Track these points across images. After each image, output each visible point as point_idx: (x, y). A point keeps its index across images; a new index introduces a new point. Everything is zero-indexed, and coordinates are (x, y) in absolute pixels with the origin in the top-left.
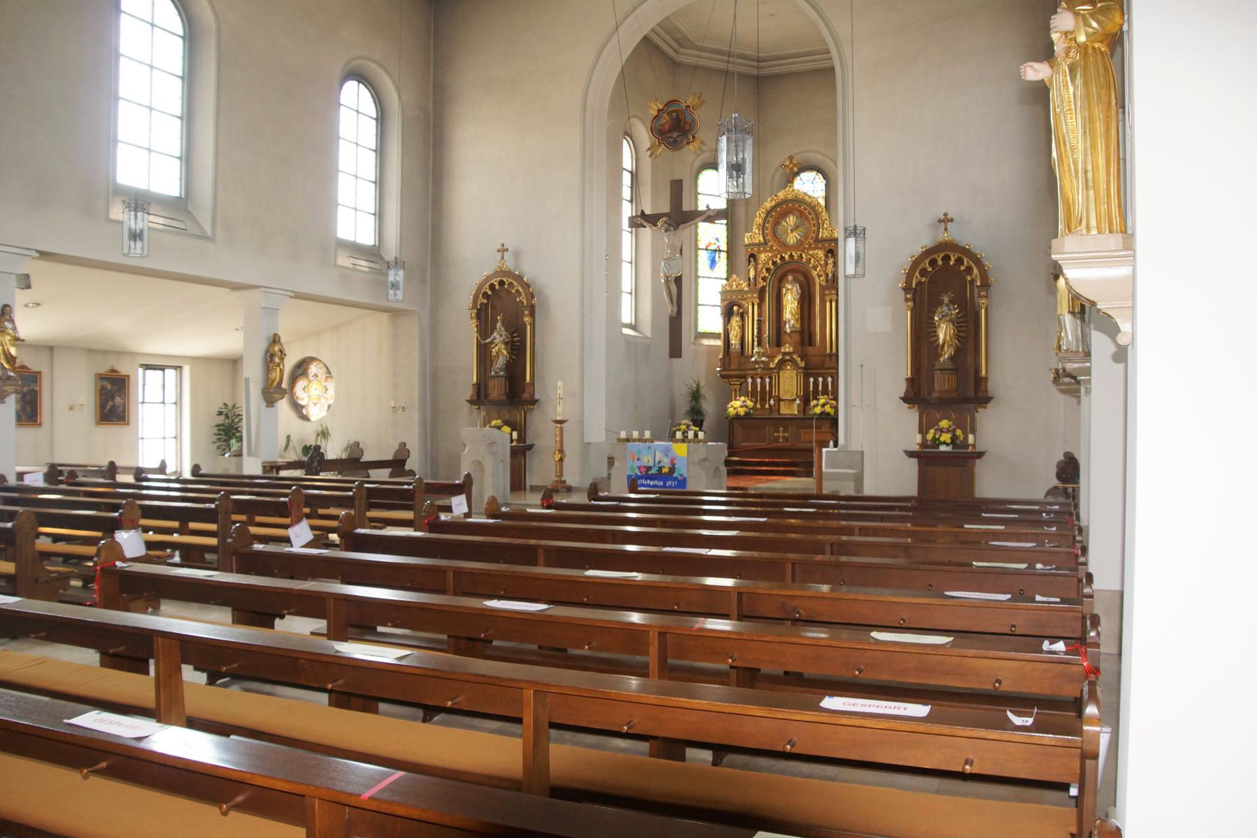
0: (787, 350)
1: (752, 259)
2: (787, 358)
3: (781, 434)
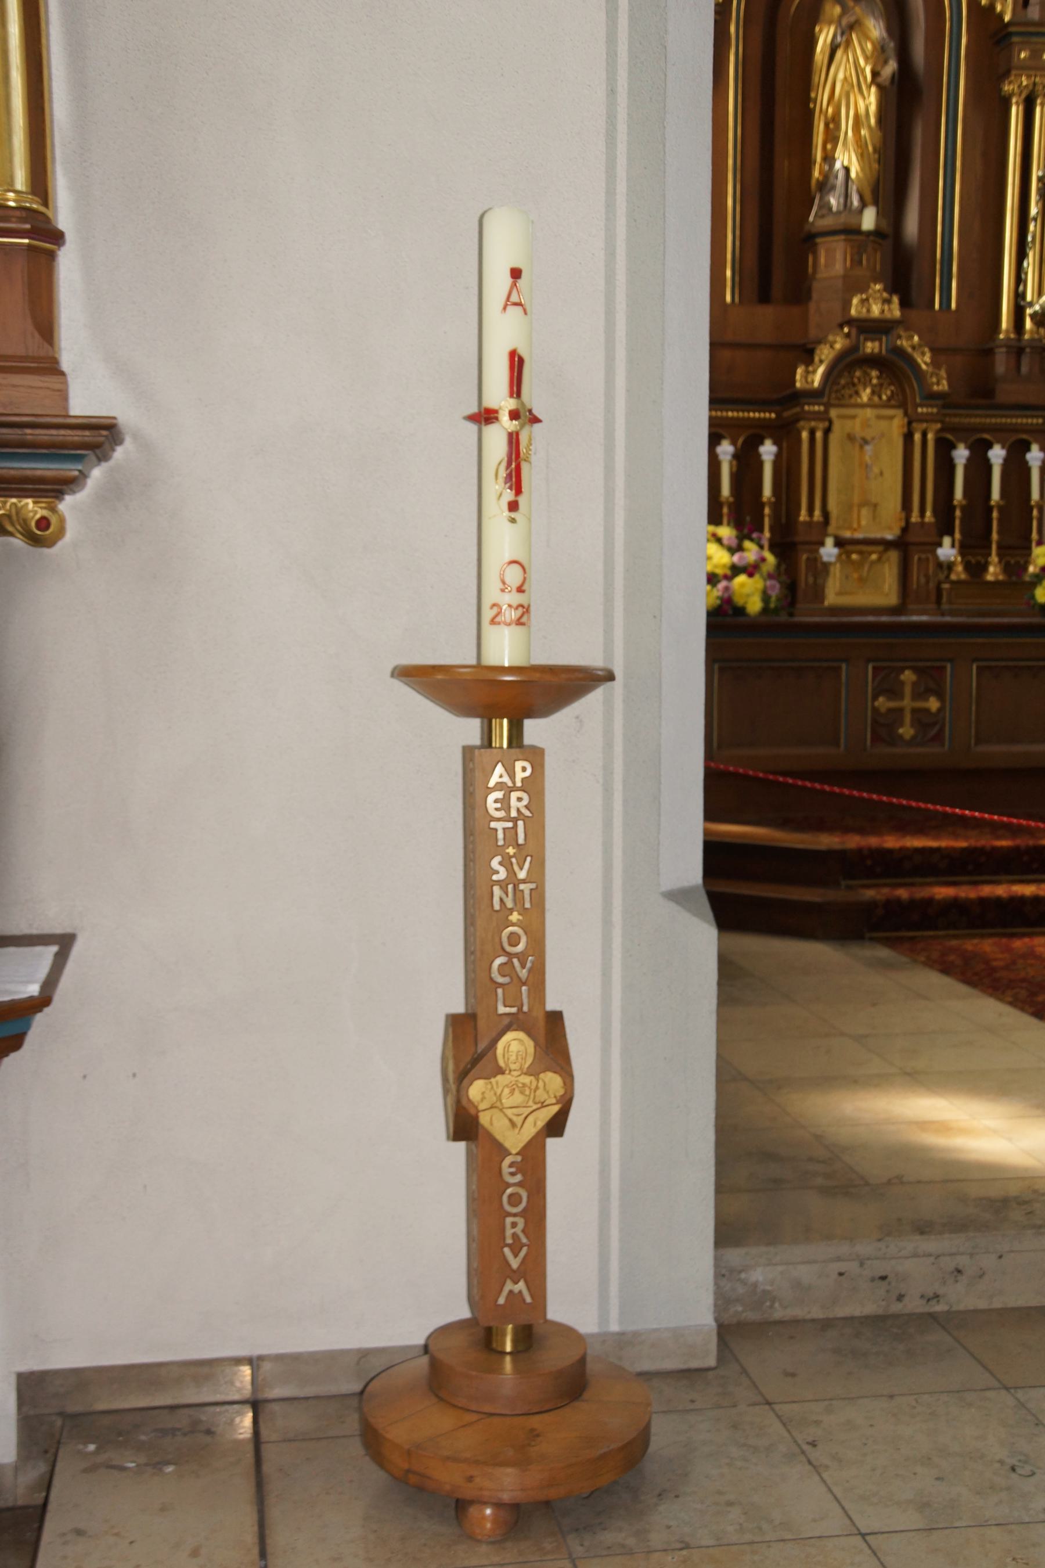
0: (876, 310)
2: (871, 347)
3: (907, 703)
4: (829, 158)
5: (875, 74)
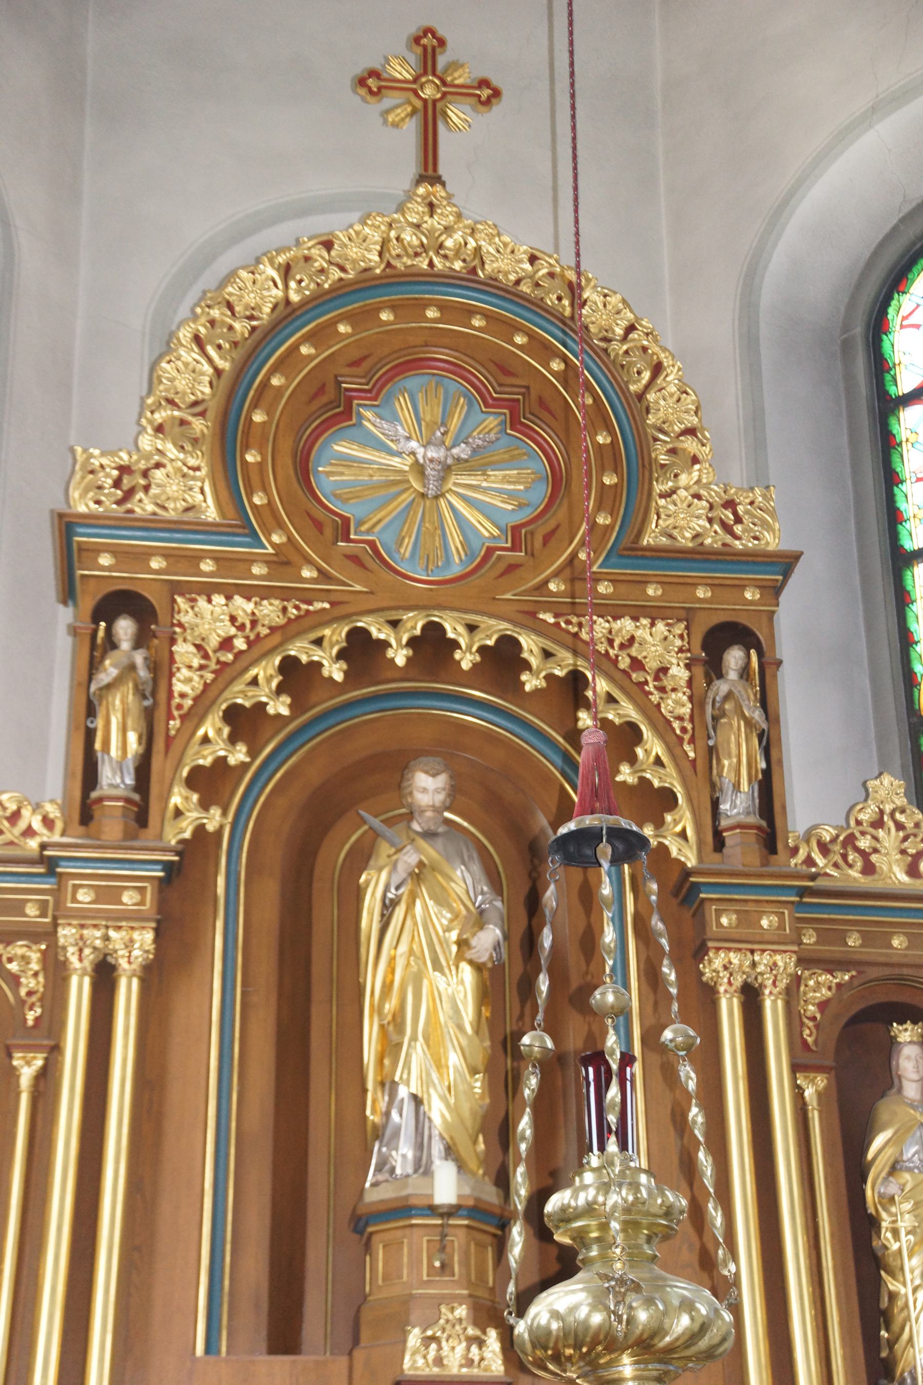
1: (125, 627)
4: (388, 1085)
5: (462, 944)
